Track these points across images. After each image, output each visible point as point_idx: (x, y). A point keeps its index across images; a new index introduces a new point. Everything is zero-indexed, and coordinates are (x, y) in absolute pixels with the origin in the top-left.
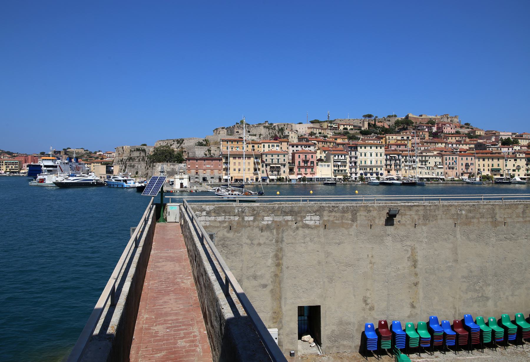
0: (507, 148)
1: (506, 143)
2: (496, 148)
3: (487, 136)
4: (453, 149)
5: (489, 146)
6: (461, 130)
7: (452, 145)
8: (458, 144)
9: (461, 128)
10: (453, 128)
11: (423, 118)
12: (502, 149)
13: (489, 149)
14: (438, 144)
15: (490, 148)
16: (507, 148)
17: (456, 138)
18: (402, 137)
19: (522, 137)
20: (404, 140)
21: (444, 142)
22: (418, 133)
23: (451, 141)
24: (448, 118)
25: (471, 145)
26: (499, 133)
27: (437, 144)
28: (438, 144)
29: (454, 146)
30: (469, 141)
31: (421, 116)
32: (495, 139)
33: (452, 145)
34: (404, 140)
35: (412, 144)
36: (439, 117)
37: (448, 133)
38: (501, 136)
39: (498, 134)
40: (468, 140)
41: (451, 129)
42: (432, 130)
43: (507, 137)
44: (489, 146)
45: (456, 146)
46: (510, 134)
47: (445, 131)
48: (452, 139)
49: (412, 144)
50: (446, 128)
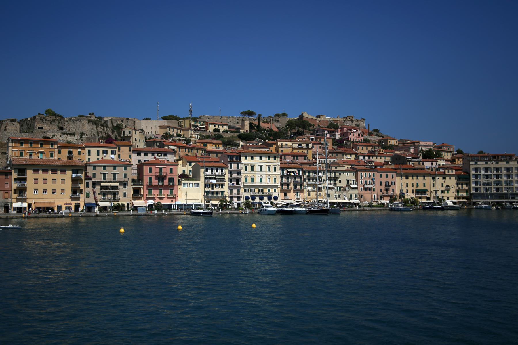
0: (431, 163)
1: (428, 156)
2: (417, 162)
4: (366, 163)
5: (410, 160)
6: (370, 137)
7: (364, 158)
8: (371, 156)
9: (370, 135)
10: (361, 135)
11: (321, 120)
12: (425, 163)
13: (409, 163)
14: (346, 156)
15: (411, 163)
16: (431, 163)
18: (300, 145)
19: (442, 148)
20: (302, 148)
22: (319, 139)
23: (362, 151)
24: (352, 121)
25: (387, 158)
26: (419, 143)
27: (345, 155)
28: (346, 156)
29: (367, 158)
30: (383, 152)
31: (319, 116)
32: (414, 150)
33: (364, 158)
34: (302, 148)
35: (312, 154)
36: (341, 120)
37: (355, 140)
38: (421, 147)
40: (382, 151)
41: (359, 135)
42: (335, 136)
43: (428, 148)
44: (410, 160)
45: (369, 158)
46: (431, 144)
47: (351, 138)
48: (362, 149)
49: (312, 154)
50: (352, 134)
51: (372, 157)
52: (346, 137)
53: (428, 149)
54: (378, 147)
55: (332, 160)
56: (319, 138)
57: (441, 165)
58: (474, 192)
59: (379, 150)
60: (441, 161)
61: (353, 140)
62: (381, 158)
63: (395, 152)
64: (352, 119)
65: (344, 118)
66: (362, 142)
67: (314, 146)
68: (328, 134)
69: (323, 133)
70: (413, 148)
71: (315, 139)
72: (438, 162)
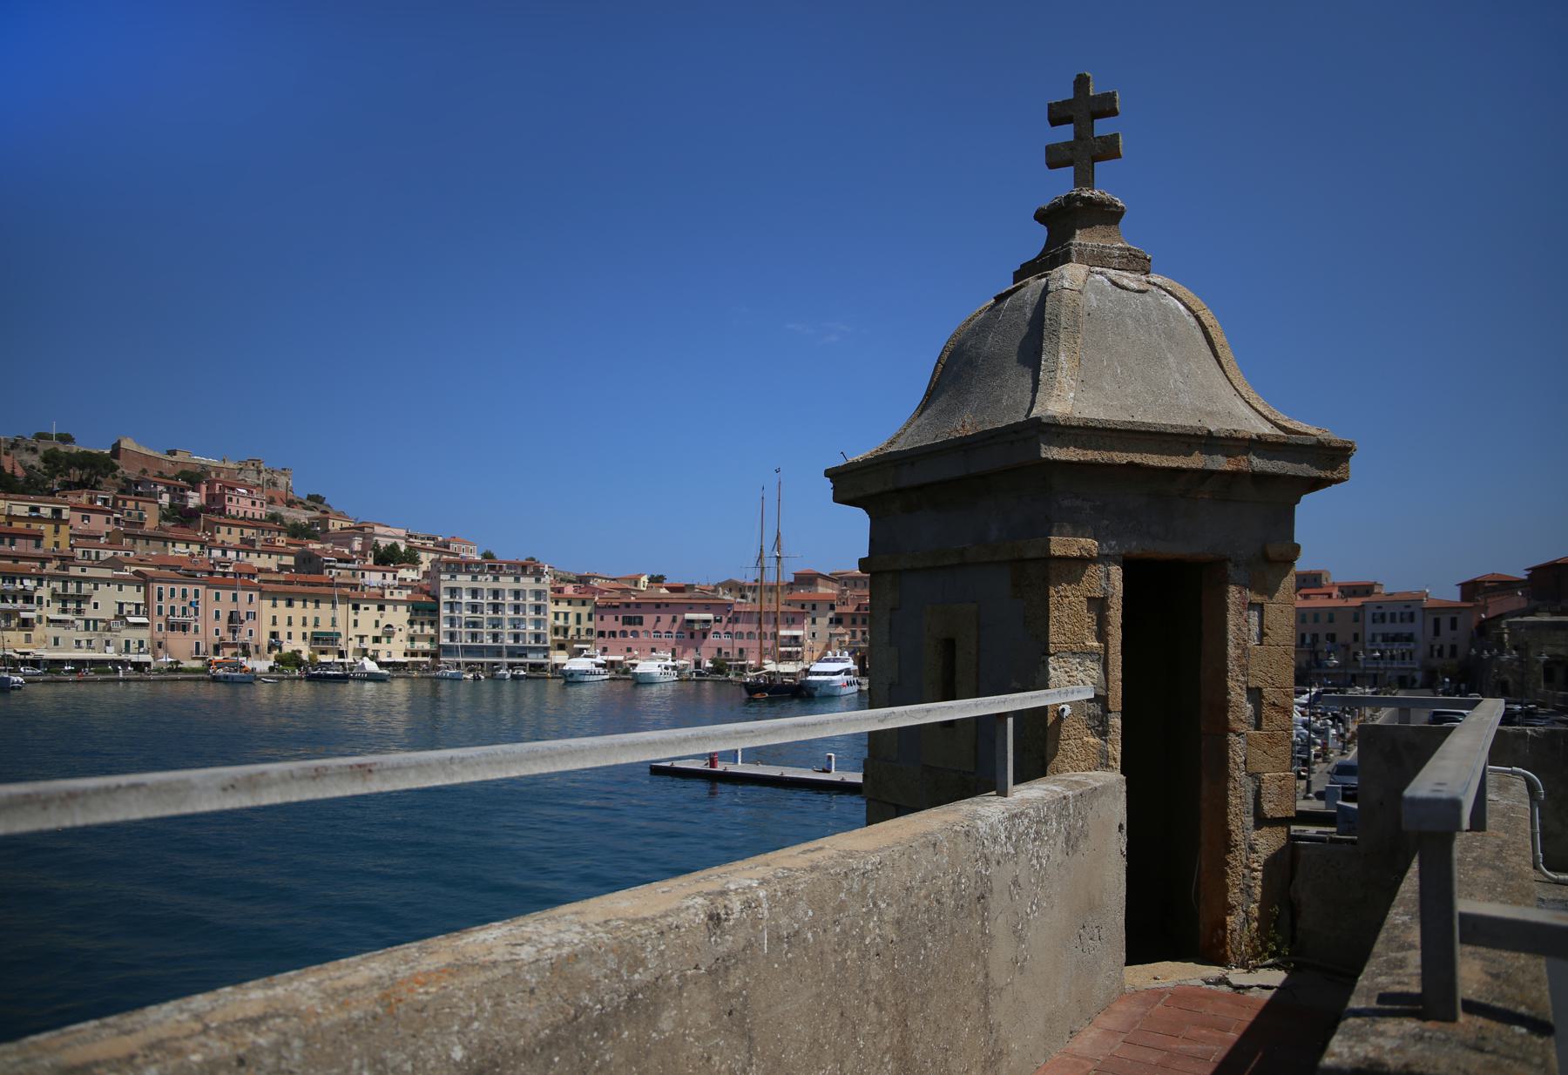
0: (381, 574)
1: (387, 558)
2: (349, 569)
3: (342, 535)
4: (213, 564)
5: (331, 564)
6: (289, 511)
7: (224, 553)
8: (243, 550)
9: (288, 506)
10: (258, 502)
11: (177, 463)
12: (367, 573)
13: (330, 573)
14: (174, 546)
15: (334, 571)
16: (381, 574)
17: (233, 529)
18: (35, 509)
19: (448, 547)
20: (40, 519)
21: (197, 539)
22: (120, 503)
23: (228, 539)
24: (259, 472)
25: (285, 558)
26: (373, 528)
27: (170, 544)
28: (174, 546)
29: (231, 555)
30: (284, 545)
31: (172, 453)
32: (363, 545)
33: (224, 553)
34: (40, 519)
35: (71, 535)
36: (232, 466)
37: (241, 515)
38: (376, 538)
39: (370, 530)
40: (281, 540)
41: (254, 504)
42: (184, 499)
43: (390, 542)
44: (331, 564)
45: (238, 555)
46: (403, 533)
47: (232, 508)
48: (229, 533)
49: (71, 535)
50: (235, 499)
51: (245, 554)
52: (219, 504)
53: (389, 544)
54: (279, 532)
55: (119, 552)
56: (120, 499)
57: (409, 580)
58: (512, 641)
59: (275, 539)
60: (408, 570)
61: (261, 517)
62: (270, 557)
63: (310, 545)
64: (257, 467)
65: (240, 462)
66: (261, 520)
67: (89, 517)
68: (166, 493)
69: (152, 490)
70: (361, 539)
71: (111, 502)
72: (397, 572)
